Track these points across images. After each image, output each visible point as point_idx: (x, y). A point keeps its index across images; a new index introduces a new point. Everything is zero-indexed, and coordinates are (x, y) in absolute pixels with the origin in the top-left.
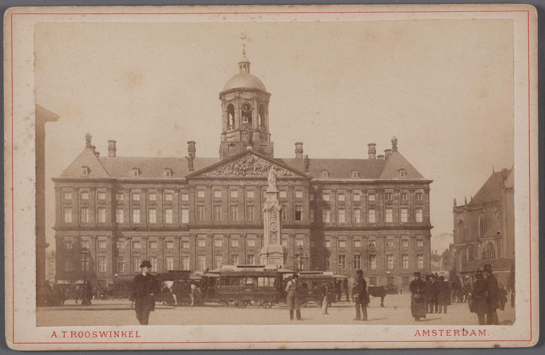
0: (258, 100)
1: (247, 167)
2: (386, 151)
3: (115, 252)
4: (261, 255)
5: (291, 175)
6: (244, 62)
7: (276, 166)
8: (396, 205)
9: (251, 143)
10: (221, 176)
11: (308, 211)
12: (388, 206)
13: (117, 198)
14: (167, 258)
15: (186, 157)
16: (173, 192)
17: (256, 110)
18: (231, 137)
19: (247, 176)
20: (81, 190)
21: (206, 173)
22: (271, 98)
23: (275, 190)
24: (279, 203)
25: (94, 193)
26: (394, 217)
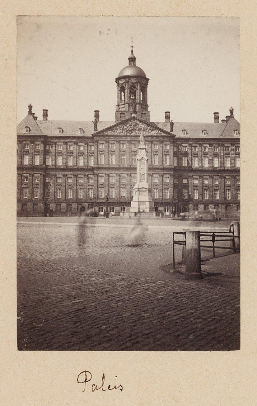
0: (140, 82)
1: (132, 128)
2: (227, 117)
4: (134, 189)
5: (161, 134)
8: (232, 155)
9: (135, 112)
10: (115, 134)
12: (227, 156)
14: (79, 189)
15: (92, 121)
16: (83, 144)
17: (139, 89)
18: (122, 108)
19: (132, 134)
21: (105, 132)
22: (149, 81)
26: (231, 164)
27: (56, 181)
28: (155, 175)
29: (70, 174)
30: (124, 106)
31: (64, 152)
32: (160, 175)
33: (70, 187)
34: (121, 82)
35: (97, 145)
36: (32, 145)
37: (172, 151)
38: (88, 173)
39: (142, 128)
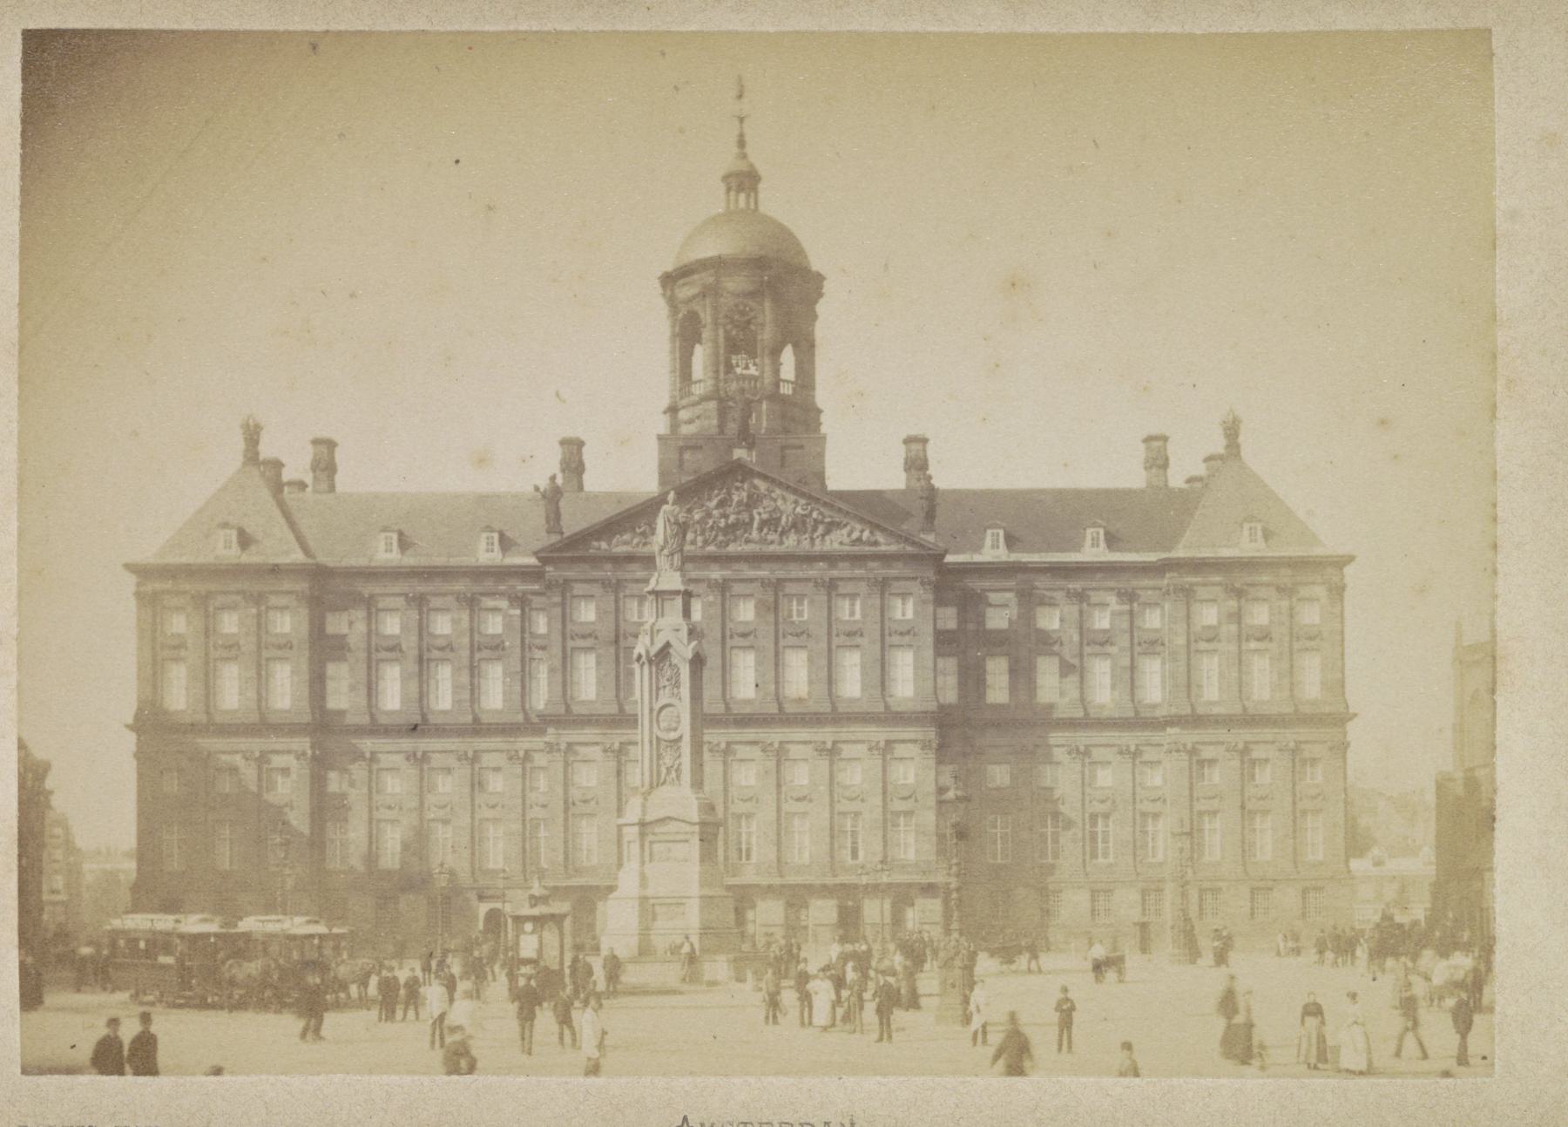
1: (732, 518)
2: (1207, 460)
5: (876, 543)
7: (827, 512)
9: (746, 437)
11: (930, 664)
15: (537, 489)
16: (503, 604)
17: (768, 328)
18: (690, 422)
19: (733, 548)
21: (598, 540)
25: (254, 611)
27: (373, 787)
30: (698, 410)
31: (410, 643)
32: (870, 749)
33: (441, 814)
35: (563, 605)
36: (254, 611)
37: (930, 629)
38: (526, 746)
39: (779, 519)
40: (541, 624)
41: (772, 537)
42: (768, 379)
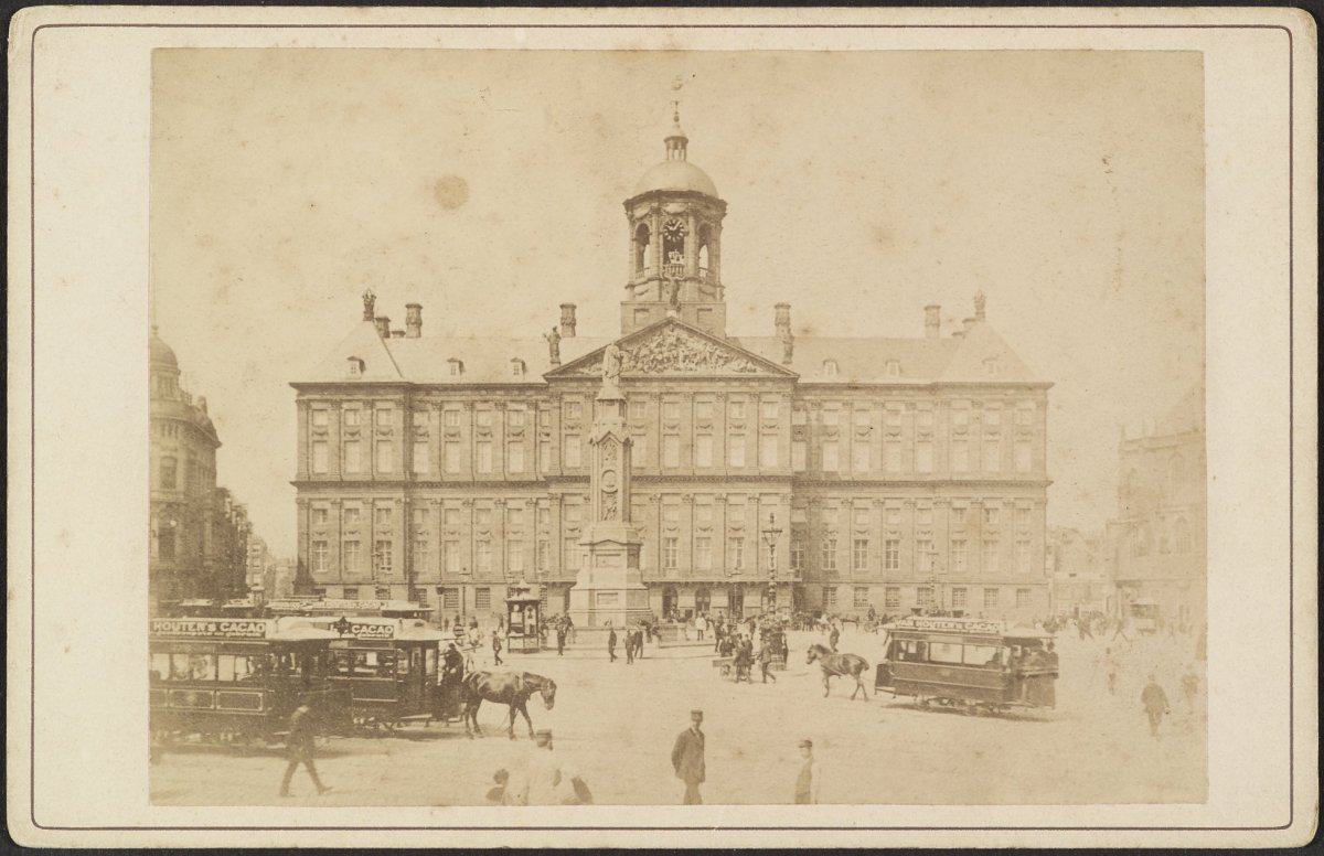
0: (696, 214)
1: (666, 354)
2: (967, 320)
3: (411, 533)
5: (755, 371)
6: (673, 138)
13: (416, 423)
16: (523, 407)
18: (642, 294)
19: (669, 373)
20: (345, 406)
23: (617, 395)
24: (624, 425)
25: (370, 412)
28: (733, 500)
29: (486, 498)
31: (465, 432)
34: (640, 212)
36: (370, 412)
38: (539, 495)
40: (546, 419)
41: (693, 366)
42: (691, 262)
